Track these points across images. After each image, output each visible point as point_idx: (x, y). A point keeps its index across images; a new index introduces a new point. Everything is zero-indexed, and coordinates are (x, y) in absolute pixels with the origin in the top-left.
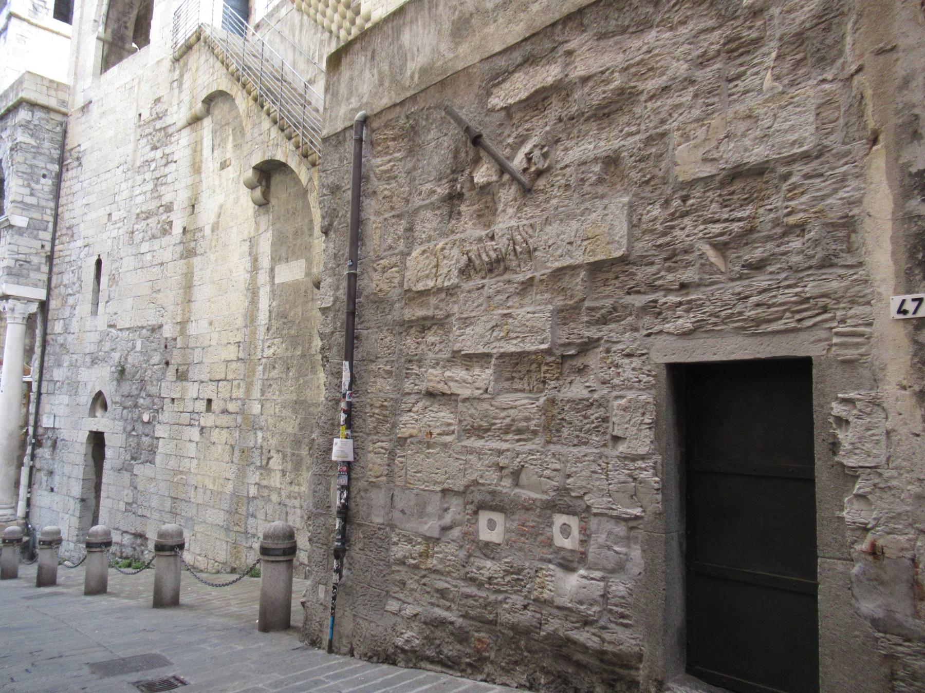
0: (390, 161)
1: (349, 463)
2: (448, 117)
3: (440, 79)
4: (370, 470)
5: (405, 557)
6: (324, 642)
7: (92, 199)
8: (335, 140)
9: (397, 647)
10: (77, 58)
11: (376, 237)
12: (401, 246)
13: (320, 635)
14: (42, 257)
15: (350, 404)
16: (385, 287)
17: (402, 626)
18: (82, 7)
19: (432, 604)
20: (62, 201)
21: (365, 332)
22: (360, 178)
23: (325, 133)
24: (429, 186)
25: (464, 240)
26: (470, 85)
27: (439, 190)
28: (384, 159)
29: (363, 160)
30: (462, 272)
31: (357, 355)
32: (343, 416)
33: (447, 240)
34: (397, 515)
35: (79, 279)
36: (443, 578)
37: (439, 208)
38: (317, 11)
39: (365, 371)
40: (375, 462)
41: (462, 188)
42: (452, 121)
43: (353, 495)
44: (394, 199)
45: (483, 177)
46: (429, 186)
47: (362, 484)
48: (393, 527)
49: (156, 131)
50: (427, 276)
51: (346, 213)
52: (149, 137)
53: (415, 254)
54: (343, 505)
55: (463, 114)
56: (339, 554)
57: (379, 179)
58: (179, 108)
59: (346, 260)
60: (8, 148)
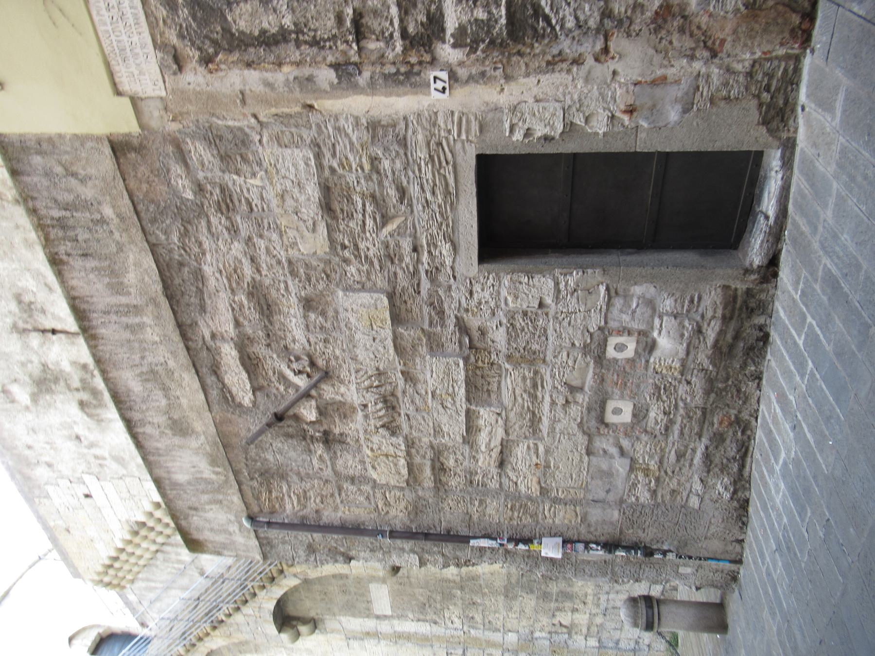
0: (290, 497)
1: (564, 542)
2: (256, 442)
3: (221, 448)
4: (571, 522)
5: (649, 490)
6: (733, 569)
8: (266, 546)
9: (732, 498)
11: (357, 511)
12: (367, 488)
13: (726, 572)
15: (510, 540)
16: (403, 504)
17: (712, 494)
19: (691, 465)
21: (443, 523)
22: (302, 525)
23: (258, 557)
24: (315, 462)
25: (366, 431)
26: (230, 422)
27: (319, 452)
29: (286, 521)
30: (393, 434)
31: (464, 532)
32: (521, 547)
33: (365, 447)
34: (611, 497)
36: (667, 455)
37: (335, 453)
39: (479, 524)
40: (563, 517)
41: (319, 432)
42: (260, 438)
43: (593, 539)
44: (324, 493)
45: (311, 412)
46: (315, 462)
47: (583, 530)
48: (622, 501)
50: (396, 465)
51: (333, 539)
53: (375, 476)
54: (603, 547)
55: (254, 429)
56: (649, 553)
57: (305, 507)
59: (377, 540)
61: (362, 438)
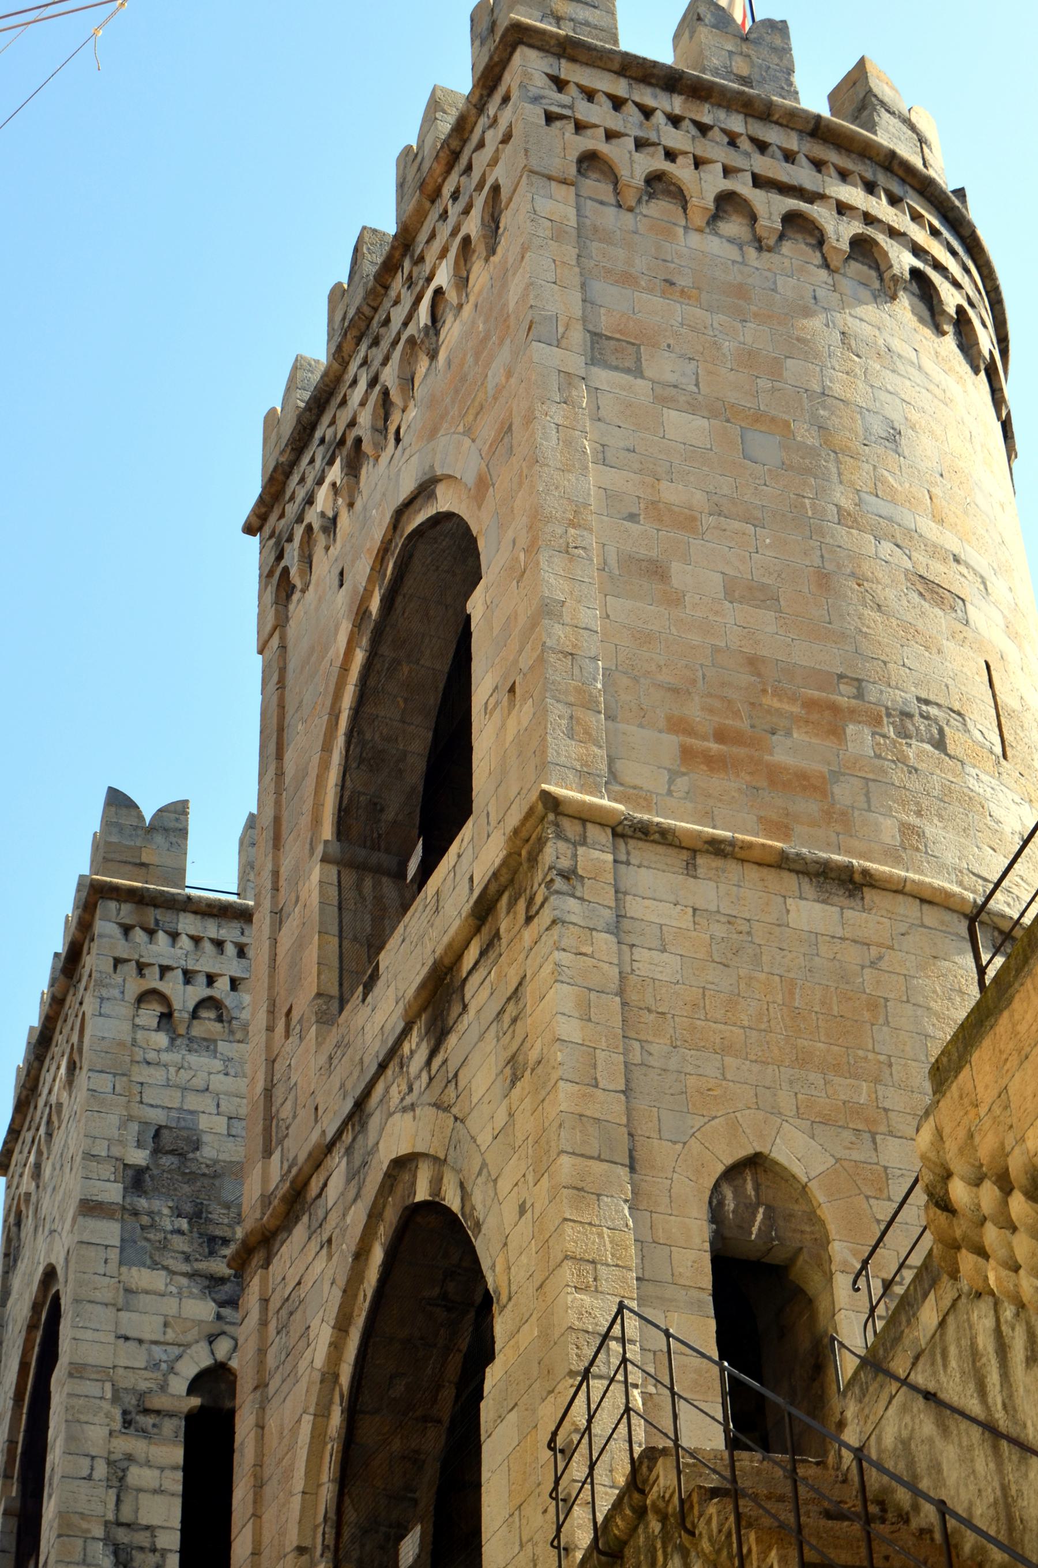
18: (256, 1516)
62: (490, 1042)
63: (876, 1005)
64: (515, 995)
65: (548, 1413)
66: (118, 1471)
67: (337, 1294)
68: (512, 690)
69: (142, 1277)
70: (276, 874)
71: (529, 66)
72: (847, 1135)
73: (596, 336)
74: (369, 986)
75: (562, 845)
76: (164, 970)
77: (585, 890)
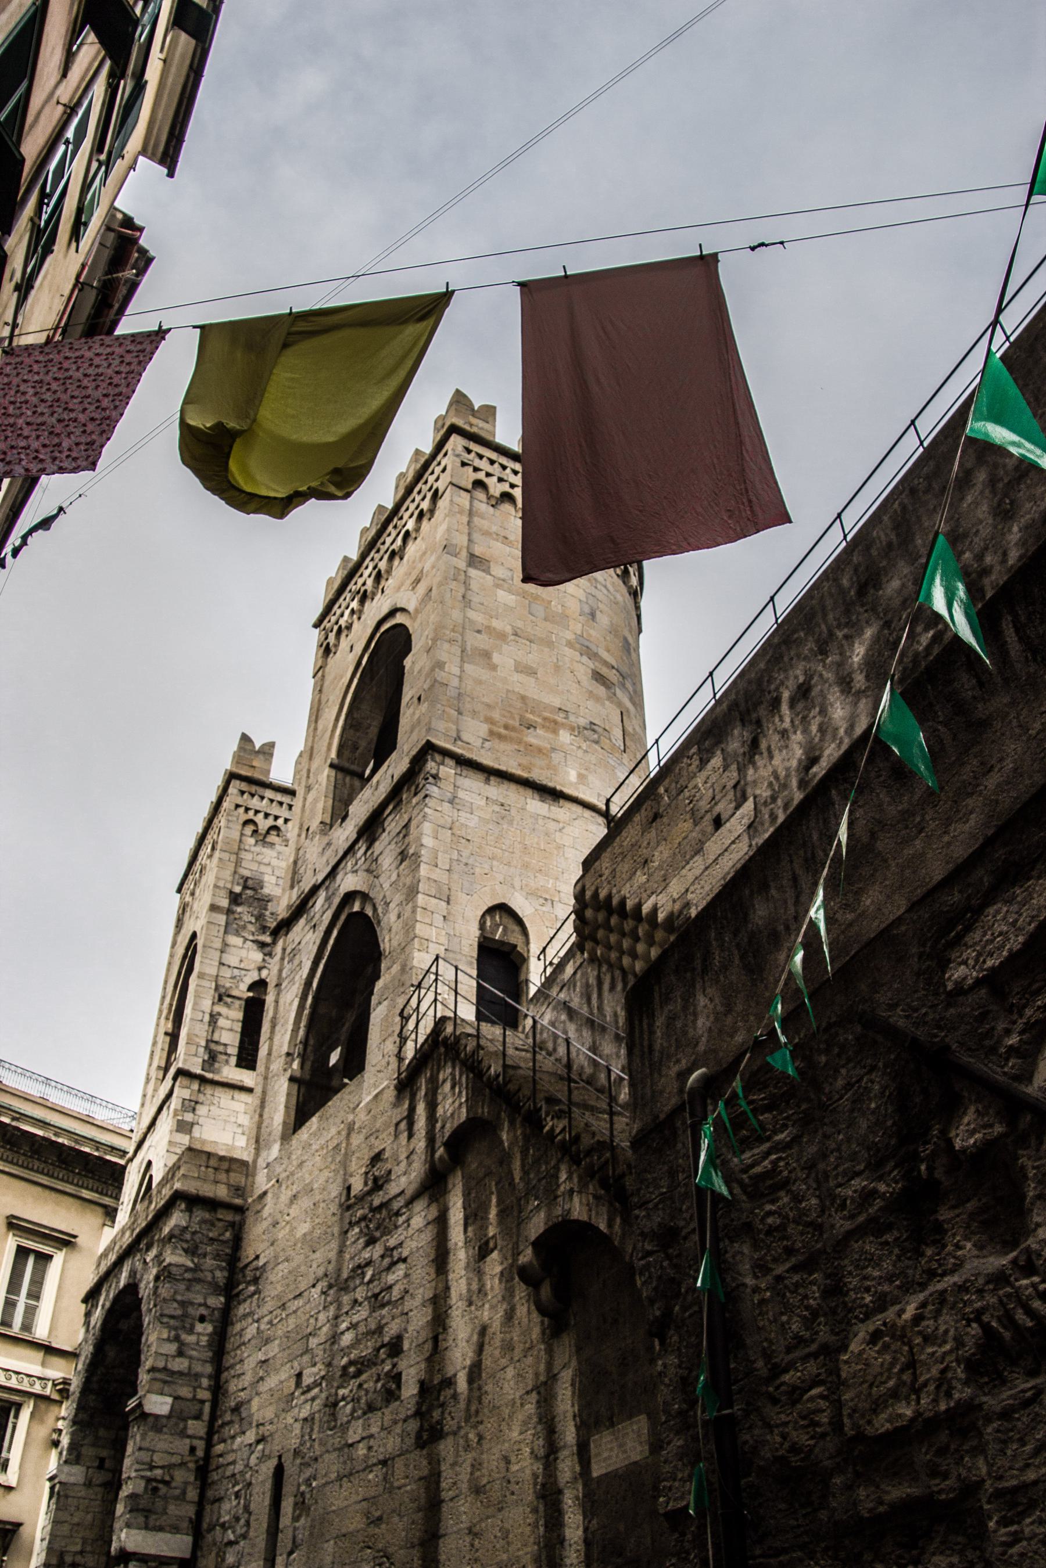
0: (768, 1153)
7: (273, 1349)
10: (261, 1116)
14: (189, 1470)
16: (803, 1439)
18: (271, 1039)
20: (228, 1361)
28: (756, 1151)
30: (973, 1367)
33: (921, 1296)
35: (247, 1509)
37: (889, 1227)
38: (622, 953)
44: (791, 1229)
45: (972, 1133)
46: (857, 1183)
49: (373, 1210)
52: (363, 1224)
58: (409, 1164)
60: (152, 1277)
61: (939, 1287)
62: (393, 846)
63: (560, 847)
64: (406, 826)
65: (401, 1001)
66: (214, 1018)
67: (316, 948)
68: (419, 699)
69: (234, 940)
70: (309, 771)
71: (456, 442)
72: (542, 901)
73: (472, 556)
74: (344, 819)
75: (433, 764)
76: (257, 812)
77: (441, 784)
